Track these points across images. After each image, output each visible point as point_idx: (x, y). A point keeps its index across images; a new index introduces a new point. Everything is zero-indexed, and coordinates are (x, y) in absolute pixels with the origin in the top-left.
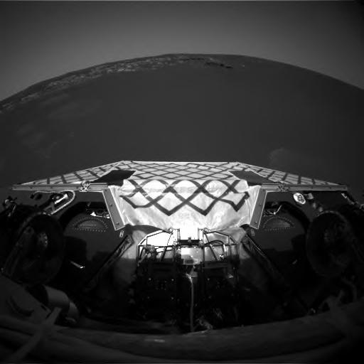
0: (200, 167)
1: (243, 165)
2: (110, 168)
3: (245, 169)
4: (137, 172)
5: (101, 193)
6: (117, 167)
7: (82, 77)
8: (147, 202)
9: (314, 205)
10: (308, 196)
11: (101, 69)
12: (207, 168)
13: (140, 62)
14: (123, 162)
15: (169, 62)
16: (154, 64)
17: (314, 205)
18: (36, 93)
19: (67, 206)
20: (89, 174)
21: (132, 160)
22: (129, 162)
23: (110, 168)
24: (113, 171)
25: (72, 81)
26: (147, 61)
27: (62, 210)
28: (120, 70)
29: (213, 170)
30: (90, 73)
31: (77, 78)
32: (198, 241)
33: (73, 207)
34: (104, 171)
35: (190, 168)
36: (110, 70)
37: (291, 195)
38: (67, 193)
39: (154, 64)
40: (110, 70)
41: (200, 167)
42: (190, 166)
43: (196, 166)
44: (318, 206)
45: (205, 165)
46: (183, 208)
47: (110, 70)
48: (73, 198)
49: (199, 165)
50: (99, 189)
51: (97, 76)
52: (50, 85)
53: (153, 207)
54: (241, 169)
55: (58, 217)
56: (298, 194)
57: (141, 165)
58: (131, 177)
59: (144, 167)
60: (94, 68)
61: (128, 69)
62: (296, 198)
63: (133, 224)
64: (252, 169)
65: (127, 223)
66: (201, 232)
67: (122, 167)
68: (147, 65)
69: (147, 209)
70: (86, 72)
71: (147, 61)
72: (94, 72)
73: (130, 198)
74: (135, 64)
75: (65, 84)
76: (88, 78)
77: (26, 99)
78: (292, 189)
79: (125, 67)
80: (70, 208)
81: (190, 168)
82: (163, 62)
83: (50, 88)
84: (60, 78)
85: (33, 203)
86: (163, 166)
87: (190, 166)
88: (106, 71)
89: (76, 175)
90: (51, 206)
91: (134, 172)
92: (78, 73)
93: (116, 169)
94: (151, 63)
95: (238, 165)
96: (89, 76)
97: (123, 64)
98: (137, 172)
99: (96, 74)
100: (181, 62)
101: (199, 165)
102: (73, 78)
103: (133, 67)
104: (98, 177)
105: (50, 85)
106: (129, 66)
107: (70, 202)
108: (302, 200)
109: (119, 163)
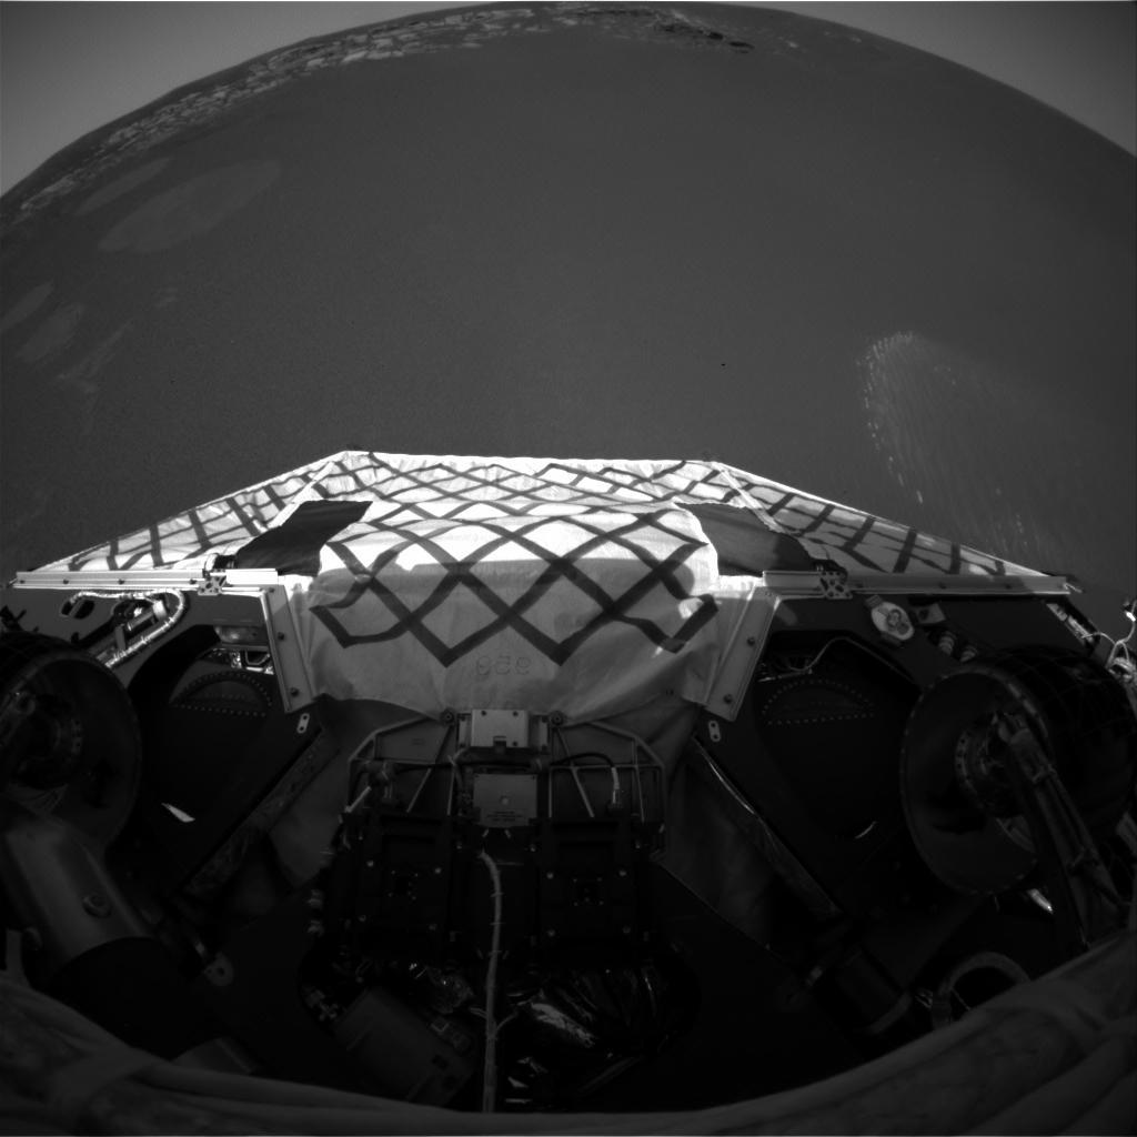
0: (587, 484)
1: (729, 475)
2: (297, 490)
3: (733, 494)
4: (378, 509)
5: (257, 600)
6: (318, 487)
7: (221, 95)
8: (391, 620)
9: (947, 644)
10: (925, 614)
11: (286, 60)
12: (603, 487)
13: (423, 25)
14: (337, 457)
15: (530, 22)
16: (472, 29)
17: (947, 644)
18: (64, 181)
19: (155, 640)
20: (234, 519)
21: (371, 443)
22: (352, 458)
23: (297, 490)
24: (306, 506)
25: (186, 113)
26: (450, 20)
27: (143, 648)
28: (354, 56)
29: (623, 493)
30: (250, 80)
31: (204, 100)
32: (531, 751)
33: (177, 639)
34: (279, 502)
35: (549, 484)
36: (319, 61)
37: (860, 605)
38: (161, 597)
39: (472, 29)
40: (319, 61)
41: (587, 484)
42: (553, 475)
43: (568, 478)
44: (957, 653)
45: (598, 476)
46: (494, 641)
47: (314, 62)
48: (177, 614)
49: (582, 474)
50: (248, 582)
51: (273, 84)
52: (113, 139)
53: (408, 638)
54: (719, 494)
55: (126, 678)
56: (890, 607)
57: (397, 474)
58: (353, 529)
59: (403, 483)
60: (262, 60)
61: (381, 50)
62: (879, 618)
63: (341, 697)
64: (755, 492)
65: (323, 691)
66: (543, 728)
67: (336, 486)
68: (453, 36)
69: (389, 644)
70: (235, 76)
71: (450, 20)
72: (261, 74)
73: (339, 614)
74: (403, 35)
75: (162, 127)
76: (239, 94)
77: (35, 203)
78: (868, 590)
79: (369, 45)
80: (170, 643)
81: (549, 484)
82: (508, 23)
83: (114, 149)
84: (149, 111)
85: (64, 628)
86: (465, 475)
87: (553, 475)
88: (301, 68)
89: (194, 519)
90: (119, 633)
91: (366, 505)
92: (204, 87)
93: (318, 497)
94: (463, 27)
95: (715, 473)
96: (242, 89)
97: (362, 38)
98: (378, 509)
99: (266, 80)
100: (571, 22)
101: (582, 474)
102: (190, 105)
103: (397, 44)
104: (252, 530)
105: (113, 139)
106: (383, 42)
107: (162, 629)
108: (903, 628)
109: (327, 464)
